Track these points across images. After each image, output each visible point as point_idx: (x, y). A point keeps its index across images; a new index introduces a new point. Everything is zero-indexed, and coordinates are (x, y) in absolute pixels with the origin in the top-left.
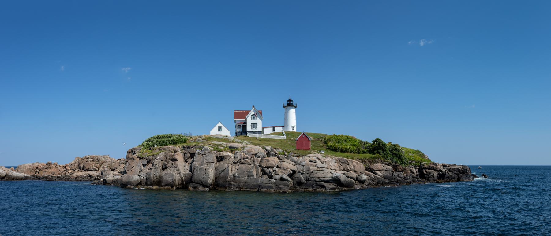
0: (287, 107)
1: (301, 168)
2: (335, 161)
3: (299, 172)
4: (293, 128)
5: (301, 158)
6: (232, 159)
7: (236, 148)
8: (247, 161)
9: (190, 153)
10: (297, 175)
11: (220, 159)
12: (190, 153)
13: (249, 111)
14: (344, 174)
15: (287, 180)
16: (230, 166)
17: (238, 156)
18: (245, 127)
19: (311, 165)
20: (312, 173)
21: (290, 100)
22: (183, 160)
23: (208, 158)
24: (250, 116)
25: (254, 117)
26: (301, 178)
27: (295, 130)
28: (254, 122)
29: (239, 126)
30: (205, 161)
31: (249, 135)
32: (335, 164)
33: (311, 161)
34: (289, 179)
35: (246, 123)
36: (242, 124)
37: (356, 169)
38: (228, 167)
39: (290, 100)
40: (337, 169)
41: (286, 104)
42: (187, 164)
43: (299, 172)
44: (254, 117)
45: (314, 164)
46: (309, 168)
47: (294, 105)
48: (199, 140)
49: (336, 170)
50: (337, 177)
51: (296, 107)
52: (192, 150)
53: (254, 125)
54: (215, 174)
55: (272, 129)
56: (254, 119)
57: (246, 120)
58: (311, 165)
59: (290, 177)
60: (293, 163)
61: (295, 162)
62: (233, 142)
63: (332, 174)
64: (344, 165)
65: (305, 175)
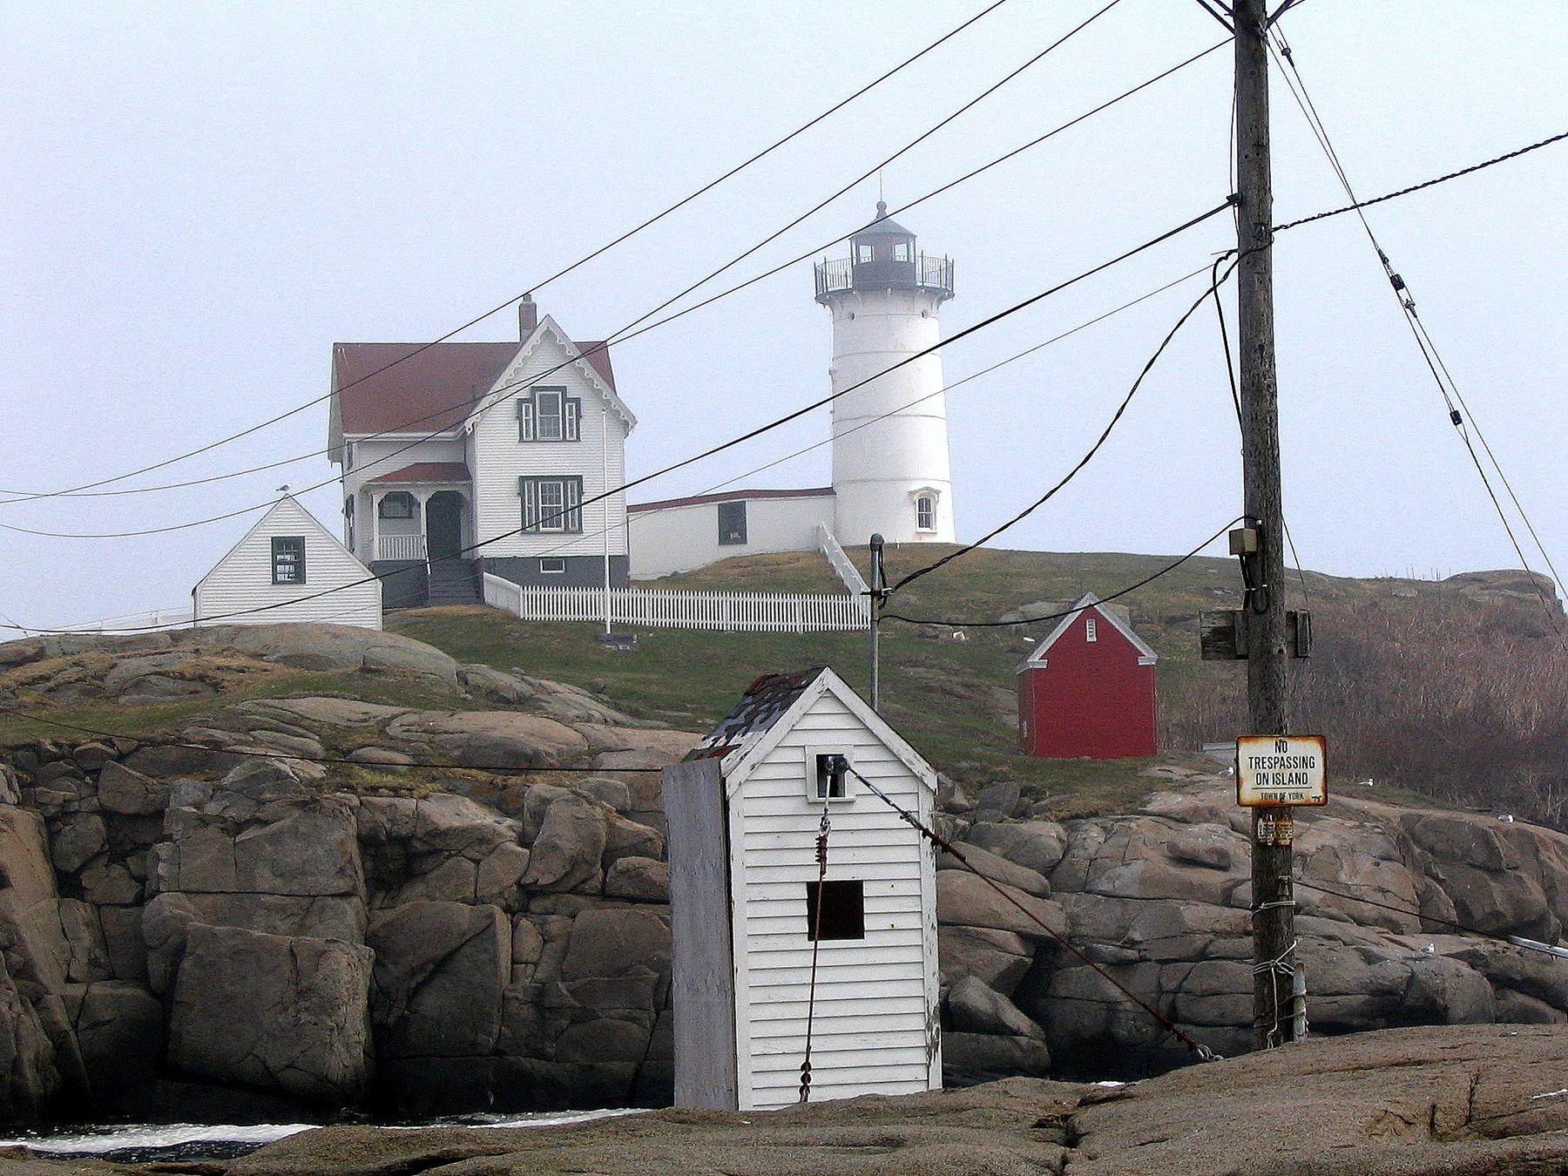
0: (850, 306)
1: (1096, 918)
2: (1380, 844)
3: (1089, 957)
4: (925, 510)
5: (1093, 834)
6: (509, 866)
7: (525, 762)
8: (636, 875)
9: (107, 814)
10: (1075, 980)
11: (395, 860)
12: (107, 814)
14: (1472, 958)
15: (999, 1028)
16: (502, 922)
17: (562, 831)
18: (451, 513)
19: (1192, 893)
20: (1202, 955)
21: (880, 232)
22: (42, 873)
23: (293, 853)
26: (1111, 1007)
28: (550, 459)
29: (397, 505)
30: (265, 879)
31: (499, 592)
33: (1187, 860)
34: (1014, 1017)
35: (462, 471)
38: (486, 932)
39: (880, 232)
40: (1410, 920)
41: (841, 276)
42: (80, 911)
43: (1089, 957)
45: (1216, 878)
46: (1176, 916)
48: (139, 683)
49: (1396, 928)
50: (1412, 977)
52: (127, 787)
54: (377, 998)
55: (711, 512)
57: (465, 441)
58: (1192, 893)
59: (1018, 1000)
60: (1034, 878)
61: (1050, 871)
62: (455, 704)
63: (1370, 958)
64: (1467, 881)
65: (1144, 980)
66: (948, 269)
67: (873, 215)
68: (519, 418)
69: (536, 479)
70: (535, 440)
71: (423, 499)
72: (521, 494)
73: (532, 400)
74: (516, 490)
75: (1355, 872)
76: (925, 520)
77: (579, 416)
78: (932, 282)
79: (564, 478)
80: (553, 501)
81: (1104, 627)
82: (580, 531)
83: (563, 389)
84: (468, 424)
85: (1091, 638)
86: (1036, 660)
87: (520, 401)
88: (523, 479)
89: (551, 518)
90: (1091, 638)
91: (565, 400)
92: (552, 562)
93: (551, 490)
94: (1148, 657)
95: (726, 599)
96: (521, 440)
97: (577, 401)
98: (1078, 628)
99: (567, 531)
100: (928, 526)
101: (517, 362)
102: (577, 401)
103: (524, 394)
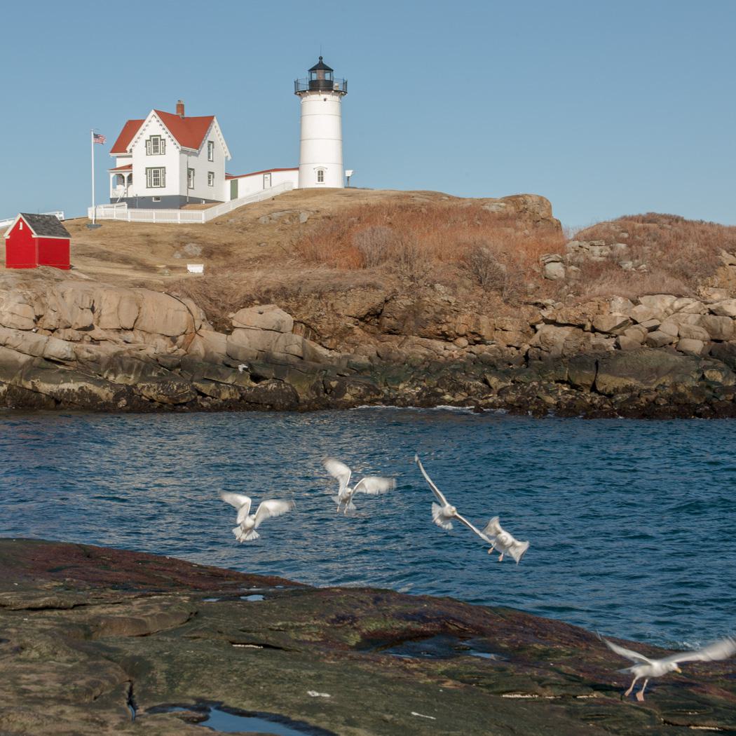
13: (140, 123)
21: (321, 67)
24: (142, 143)
25: (155, 144)
27: (333, 180)
28: (156, 161)
32: (18, 309)
35: (130, 167)
36: (126, 175)
37: (145, 324)
39: (321, 67)
41: (305, 86)
44: (155, 144)
47: (337, 85)
51: (341, 93)
53: (156, 176)
66: (345, 84)
67: (317, 62)
75: (6, 307)
76: (321, 179)
78: (340, 88)
79: (160, 168)
81: (24, 223)
84: (128, 149)
85: (21, 228)
86: (7, 236)
87: (147, 141)
88: (147, 168)
89: (157, 182)
90: (21, 228)
92: (157, 198)
94: (35, 236)
95: (154, 212)
98: (18, 225)
101: (143, 126)
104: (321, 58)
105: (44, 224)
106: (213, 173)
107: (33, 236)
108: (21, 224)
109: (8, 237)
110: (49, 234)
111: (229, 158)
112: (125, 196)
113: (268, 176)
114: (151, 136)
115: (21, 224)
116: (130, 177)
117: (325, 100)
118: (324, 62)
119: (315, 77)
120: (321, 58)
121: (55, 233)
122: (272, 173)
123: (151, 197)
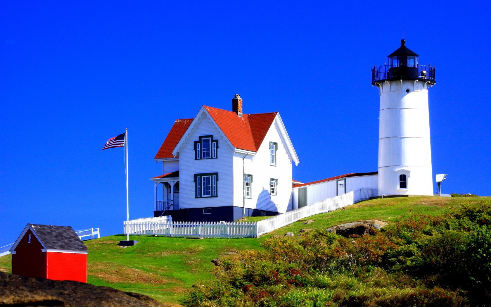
4: (403, 181)
21: (403, 53)
28: (206, 166)
39: (403, 53)
56: (206, 155)
67: (398, 46)
68: (195, 149)
69: (201, 175)
70: (201, 159)
71: (172, 185)
72: (195, 181)
73: (200, 142)
74: (193, 179)
76: (403, 185)
77: (217, 148)
80: (208, 183)
82: (217, 196)
83: (211, 136)
84: (174, 153)
88: (196, 175)
91: (212, 141)
93: (207, 180)
96: (196, 159)
97: (217, 141)
99: (212, 197)
100: (405, 187)
102: (217, 141)
103: (197, 139)
104: (403, 42)
105: (56, 237)
106: (276, 180)
107: (43, 250)
108: (30, 236)
109: (15, 253)
110: (62, 247)
111: (297, 162)
112: (172, 209)
113: (342, 182)
114: (201, 137)
115: (30, 236)
116: (177, 185)
117: (408, 91)
118: (407, 45)
119: (396, 64)
120: (403, 42)
121: (69, 247)
122: (348, 179)
123: (201, 209)
